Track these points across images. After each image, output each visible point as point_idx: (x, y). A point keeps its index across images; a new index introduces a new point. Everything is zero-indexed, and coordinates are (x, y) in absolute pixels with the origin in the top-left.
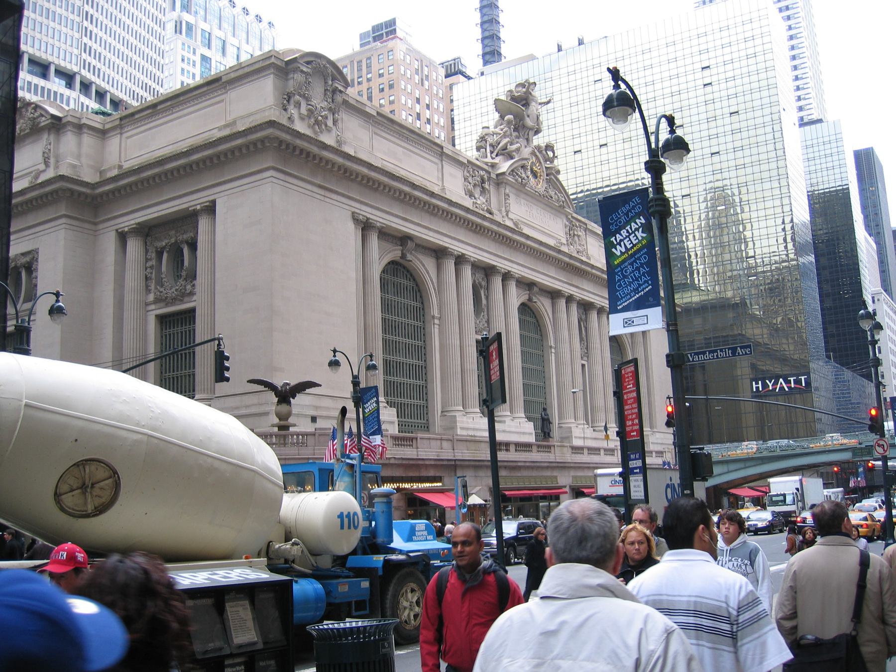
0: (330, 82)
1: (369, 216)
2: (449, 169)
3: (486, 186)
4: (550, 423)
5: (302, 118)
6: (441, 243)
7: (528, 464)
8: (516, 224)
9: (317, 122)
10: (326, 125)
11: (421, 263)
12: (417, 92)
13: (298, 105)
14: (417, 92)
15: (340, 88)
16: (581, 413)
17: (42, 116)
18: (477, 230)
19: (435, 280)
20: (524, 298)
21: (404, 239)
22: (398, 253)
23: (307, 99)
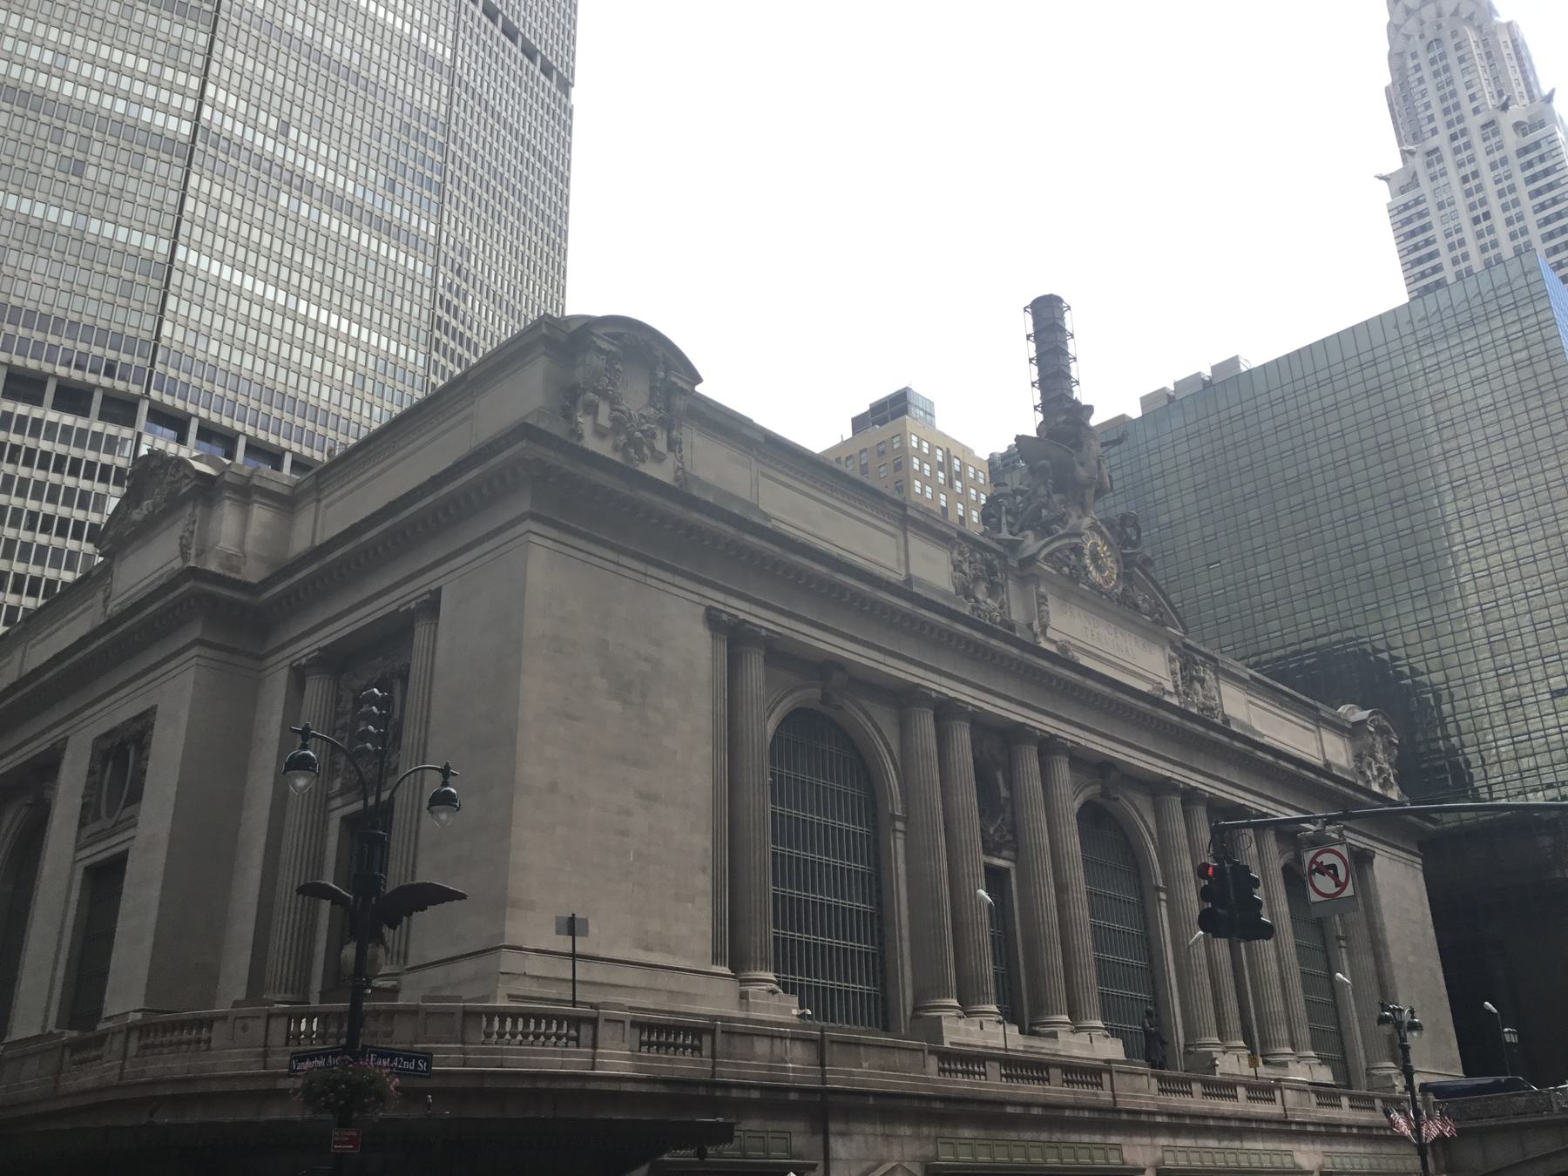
0: (661, 375)
1: (742, 616)
2: (918, 545)
3: (999, 579)
4: (1163, 1043)
5: (600, 433)
6: (903, 675)
7: (1035, 1111)
8: (1063, 649)
9: (632, 442)
10: (652, 449)
11: (866, 713)
12: (943, 497)
13: (592, 409)
14: (943, 497)
15: (681, 384)
16: (1234, 1024)
17: (186, 477)
18: (978, 654)
19: (895, 746)
20: (1092, 790)
21: (826, 668)
22: (816, 693)
23: (613, 402)
